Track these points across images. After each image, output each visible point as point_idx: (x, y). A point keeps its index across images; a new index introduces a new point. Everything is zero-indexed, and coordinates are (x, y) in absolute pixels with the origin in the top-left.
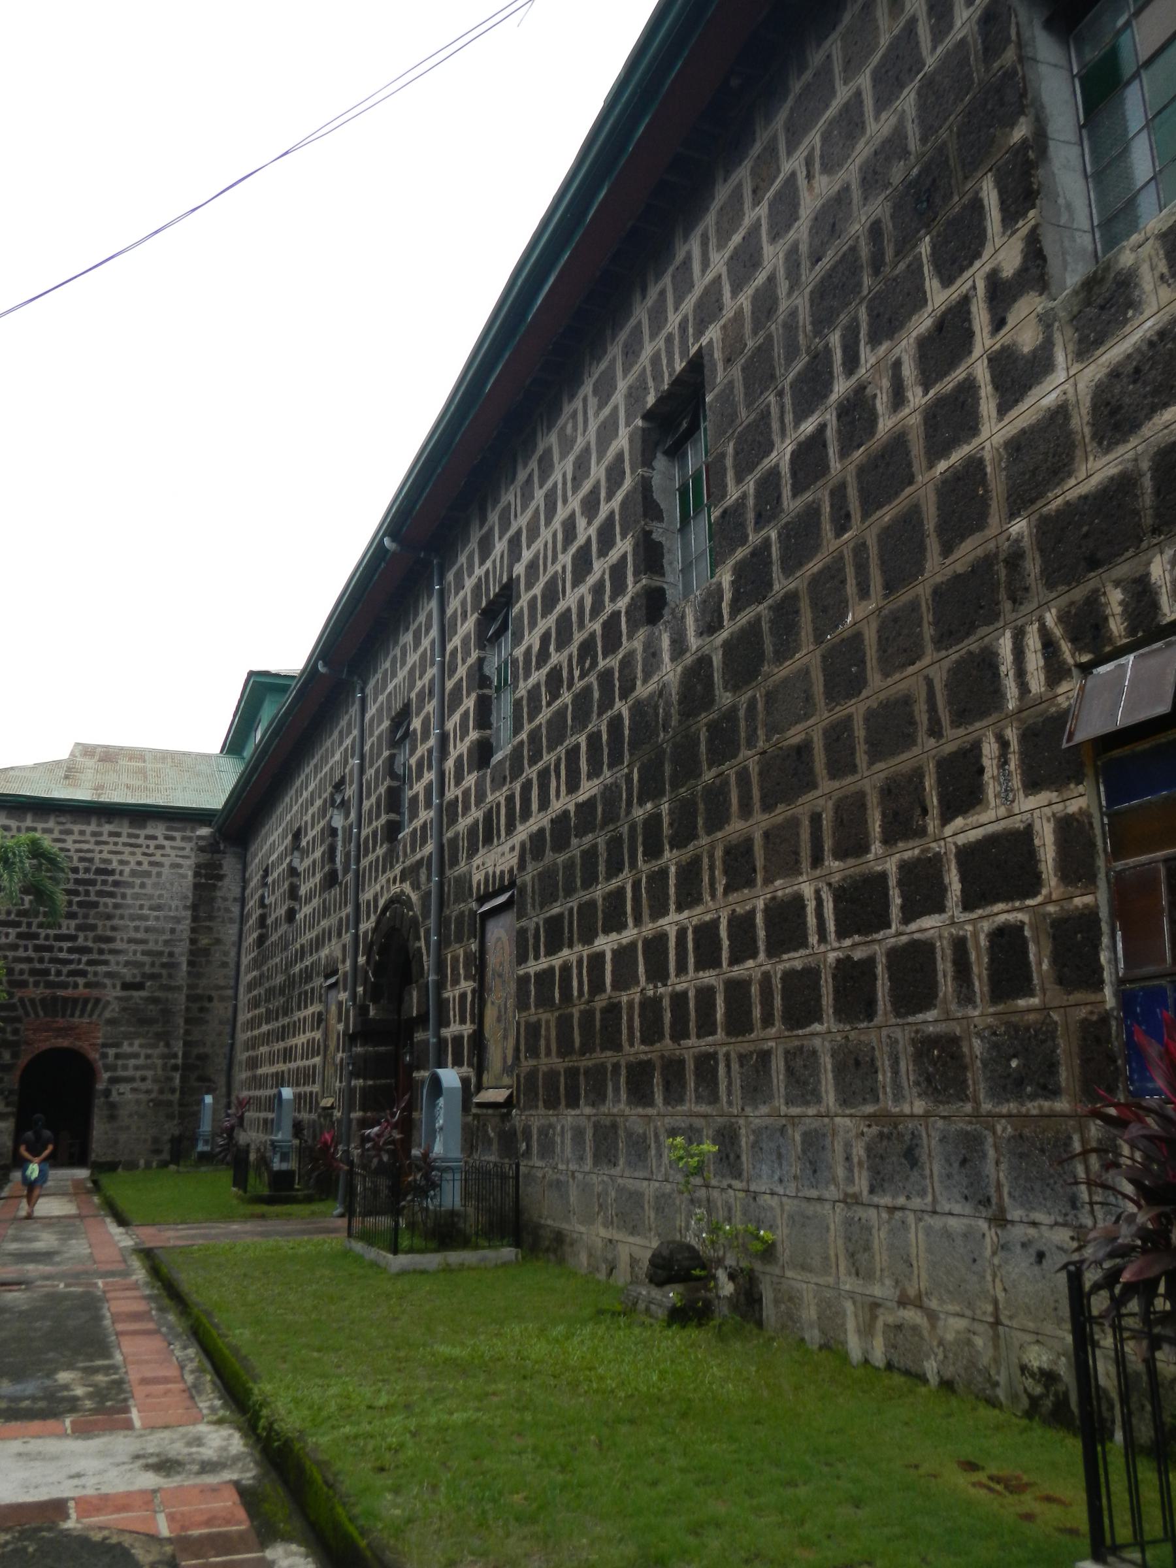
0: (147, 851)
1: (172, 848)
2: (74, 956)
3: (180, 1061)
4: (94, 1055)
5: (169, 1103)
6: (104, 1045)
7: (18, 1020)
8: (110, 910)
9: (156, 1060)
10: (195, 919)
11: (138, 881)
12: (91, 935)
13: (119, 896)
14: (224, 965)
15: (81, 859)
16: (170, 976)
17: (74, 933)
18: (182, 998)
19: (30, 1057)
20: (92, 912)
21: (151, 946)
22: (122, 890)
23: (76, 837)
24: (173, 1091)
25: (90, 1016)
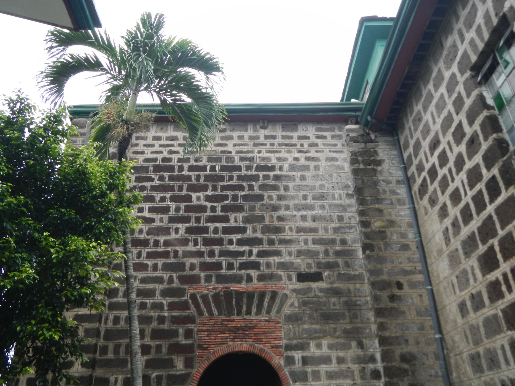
0: (301, 149)
1: (324, 145)
2: (245, 248)
3: (380, 366)
6: (288, 348)
7: (191, 320)
8: (275, 201)
9: (350, 365)
10: (361, 202)
11: (298, 175)
12: (259, 226)
13: (282, 188)
14: (405, 247)
15: (242, 159)
16: (347, 265)
17: (242, 225)
18: (366, 288)
19: (206, 364)
20: (258, 205)
21: (321, 234)
22: (284, 183)
23: (236, 141)
25: (268, 312)
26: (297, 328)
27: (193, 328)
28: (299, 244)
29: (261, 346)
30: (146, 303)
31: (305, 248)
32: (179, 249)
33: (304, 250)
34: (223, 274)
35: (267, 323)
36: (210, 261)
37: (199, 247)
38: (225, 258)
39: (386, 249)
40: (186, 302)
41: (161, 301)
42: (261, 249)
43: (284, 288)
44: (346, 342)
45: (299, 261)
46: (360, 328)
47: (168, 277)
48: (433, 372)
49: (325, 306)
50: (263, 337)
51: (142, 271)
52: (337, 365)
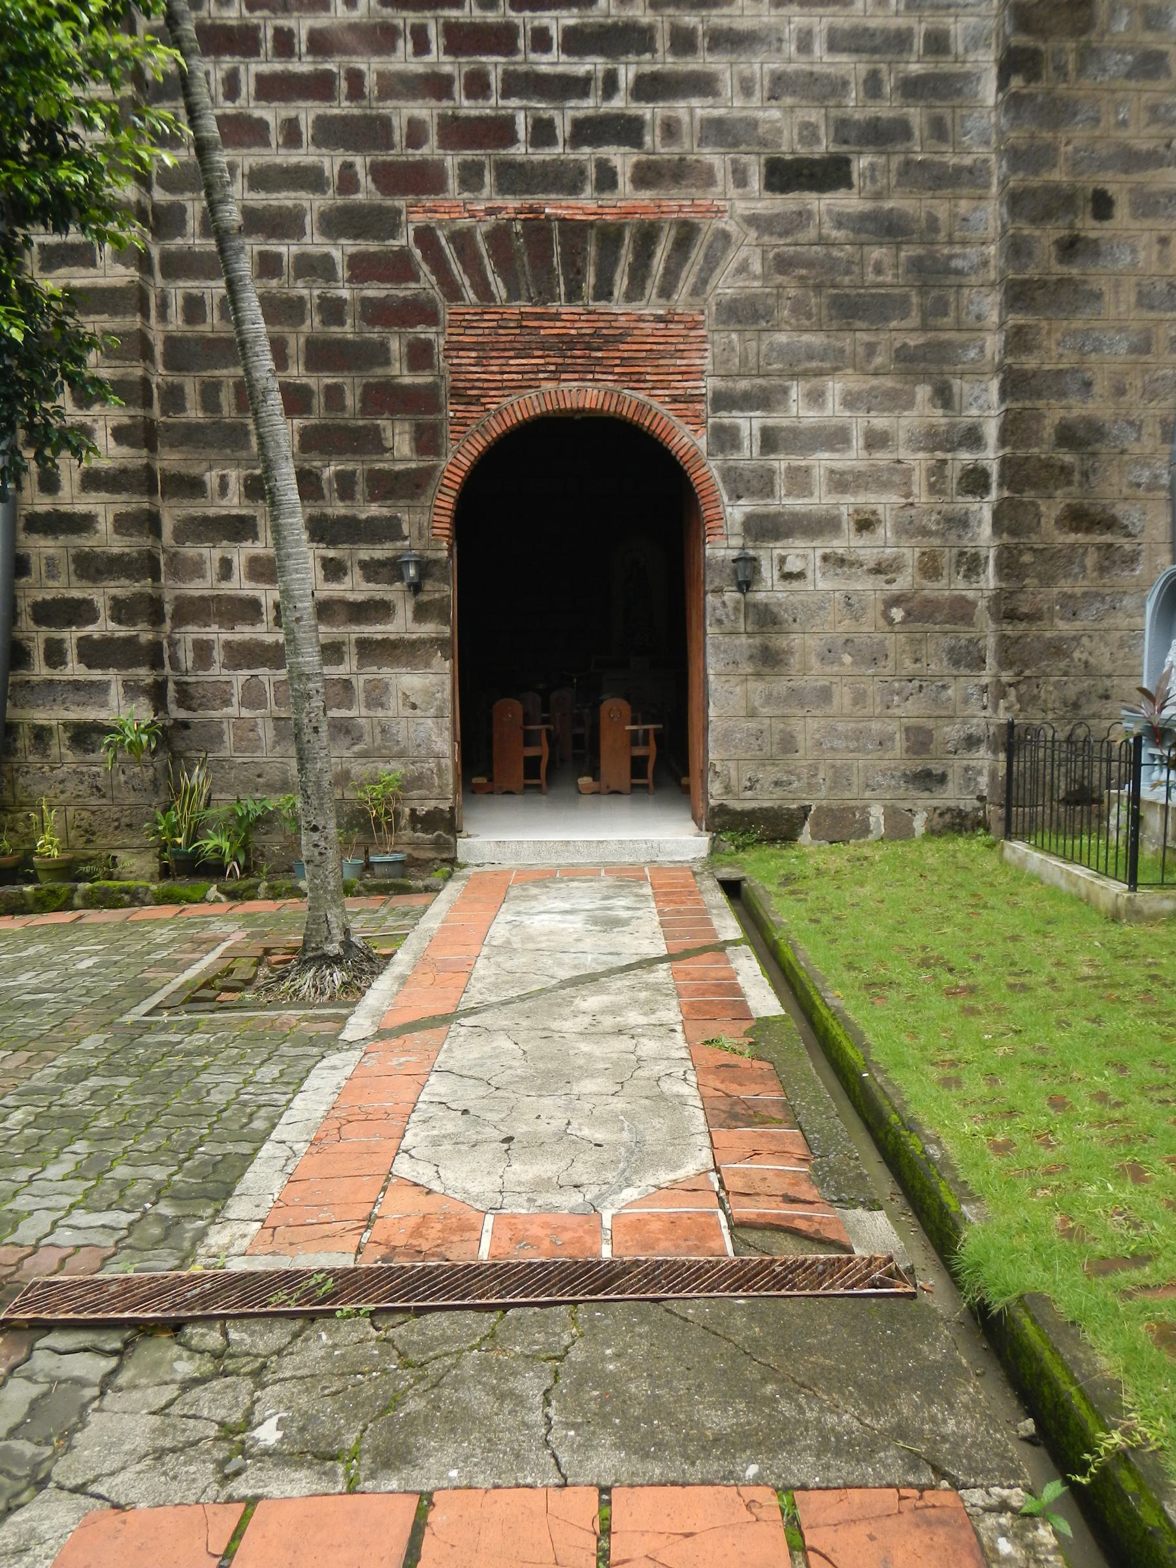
2: (591, 65)
3: (990, 457)
5: (961, 611)
6: (723, 401)
7: (424, 312)
9: (903, 454)
16: (939, 130)
19: (478, 445)
24: (972, 565)
25: (666, 292)
26: (754, 344)
27: (432, 337)
28: (779, 50)
29: (641, 396)
30: (278, 257)
31: (800, 65)
32: (363, 67)
33: (797, 74)
34: (519, 158)
35: (662, 325)
36: (474, 113)
37: (431, 58)
38: (524, 103)
39: (1081, 70)
40: (403, 255)
41: (325, 249)
42: (647, 69)
43: (720, 211)
44: (899, 386)
45: (775, 114)
46: (950, 344)
47: (337, 169)
48: (1145, 476)
49: (848, 272)
50: (649, 369)
51: (249, 147)
52: (863, 454)
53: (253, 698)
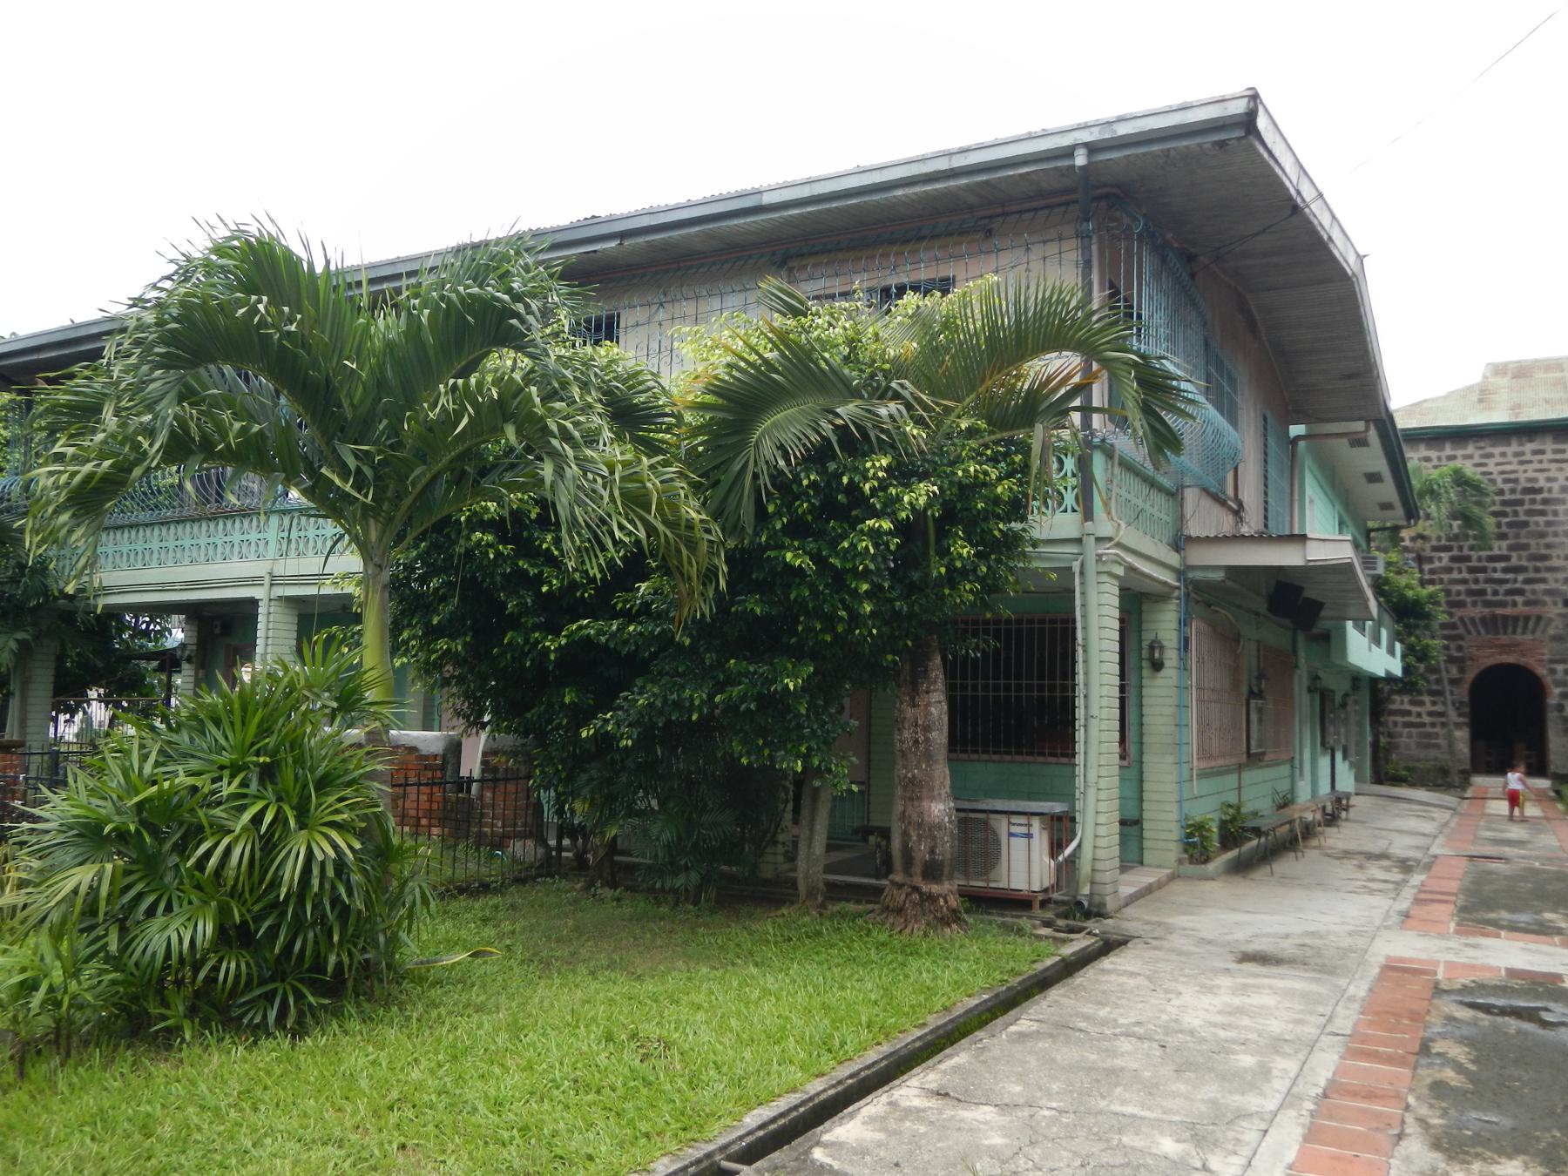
2: (1510, 576)
4: (1542, 671)
6: (1552, 661)
7: (1461, 637)
8: (1542, 528)
12: (1524, 554)
15: (1506, 481)
20: (1523, 532)
23: (1498, 459)
25: (1533, 632)
53: (1410, 736)
